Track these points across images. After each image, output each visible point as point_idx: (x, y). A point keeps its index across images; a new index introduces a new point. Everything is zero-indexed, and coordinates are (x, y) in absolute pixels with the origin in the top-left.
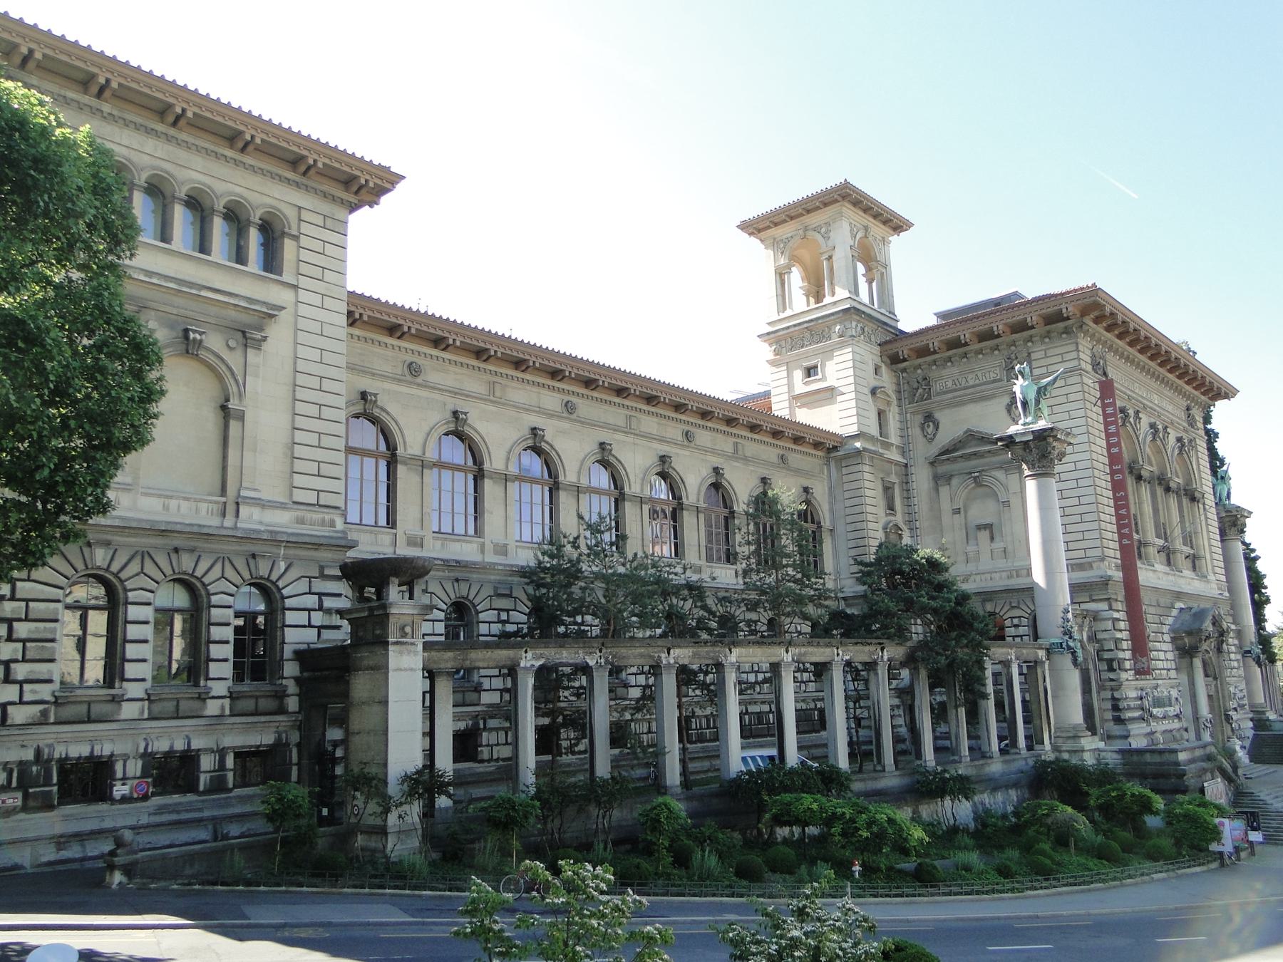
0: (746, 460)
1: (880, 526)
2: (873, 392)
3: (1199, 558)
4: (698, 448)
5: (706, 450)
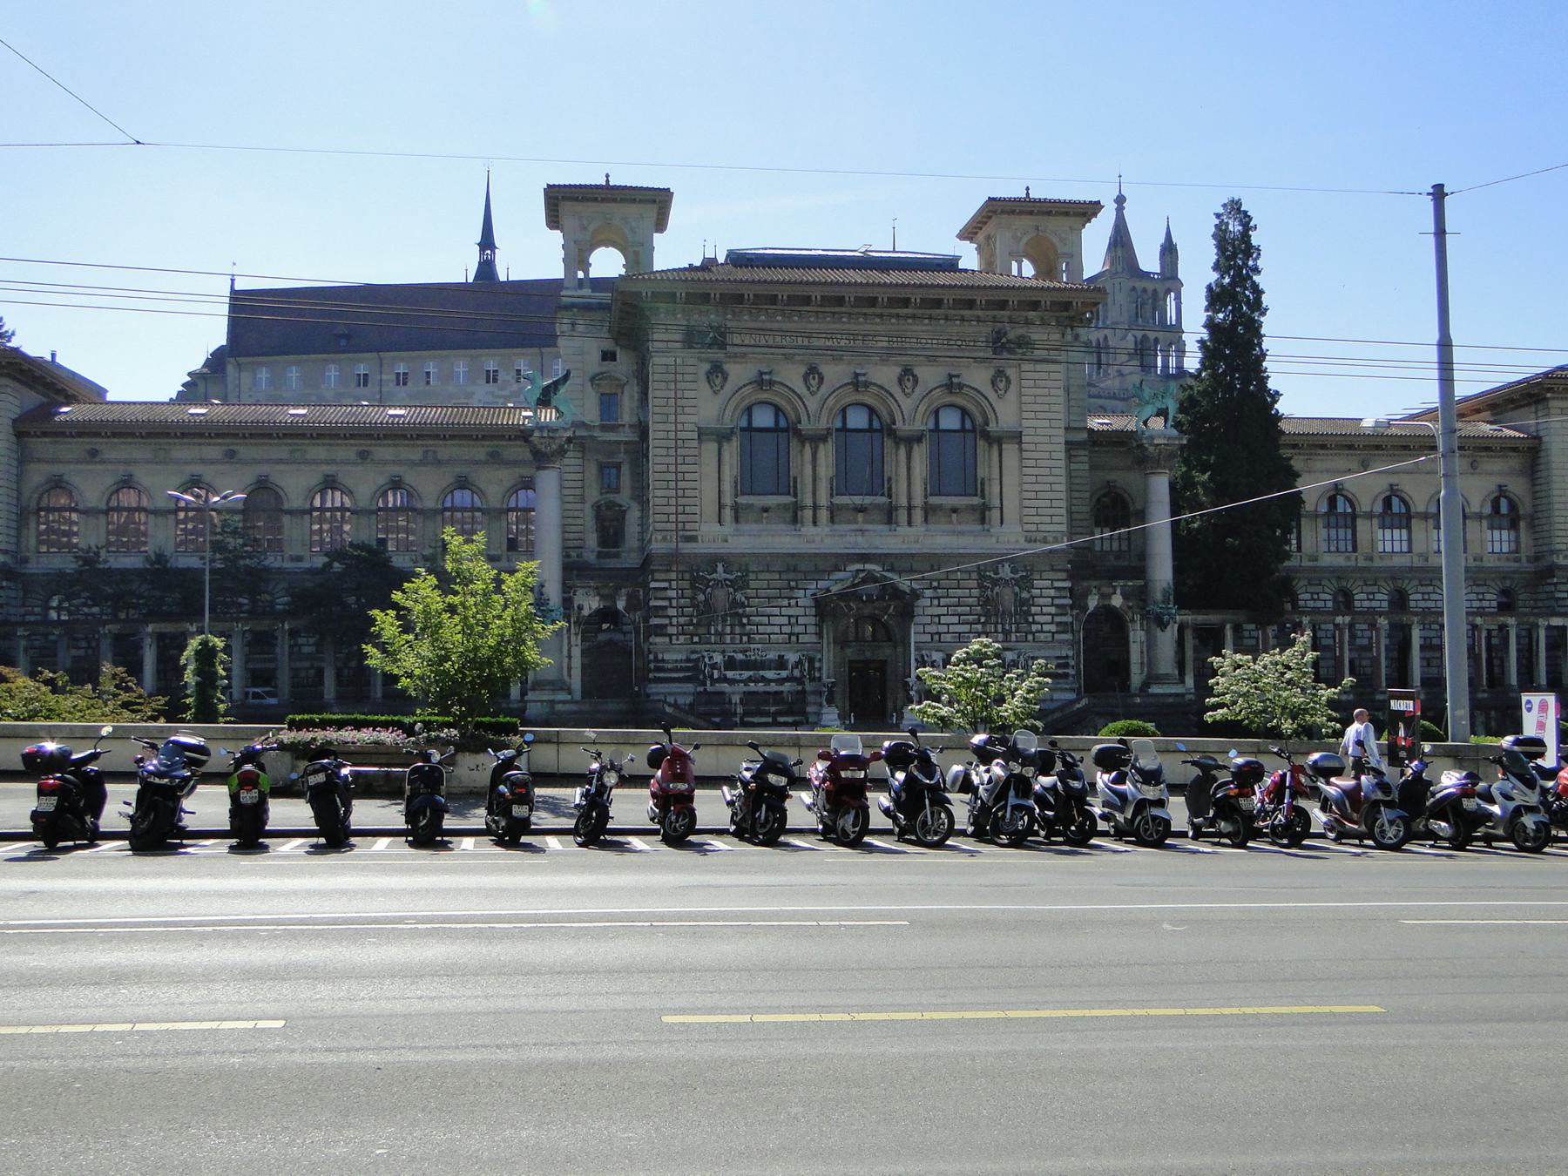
0: (438, 463)
1: (588, 508)
2: (592, 380)
3: (990, 509)
4: (374, 462)
5: (385, 462)
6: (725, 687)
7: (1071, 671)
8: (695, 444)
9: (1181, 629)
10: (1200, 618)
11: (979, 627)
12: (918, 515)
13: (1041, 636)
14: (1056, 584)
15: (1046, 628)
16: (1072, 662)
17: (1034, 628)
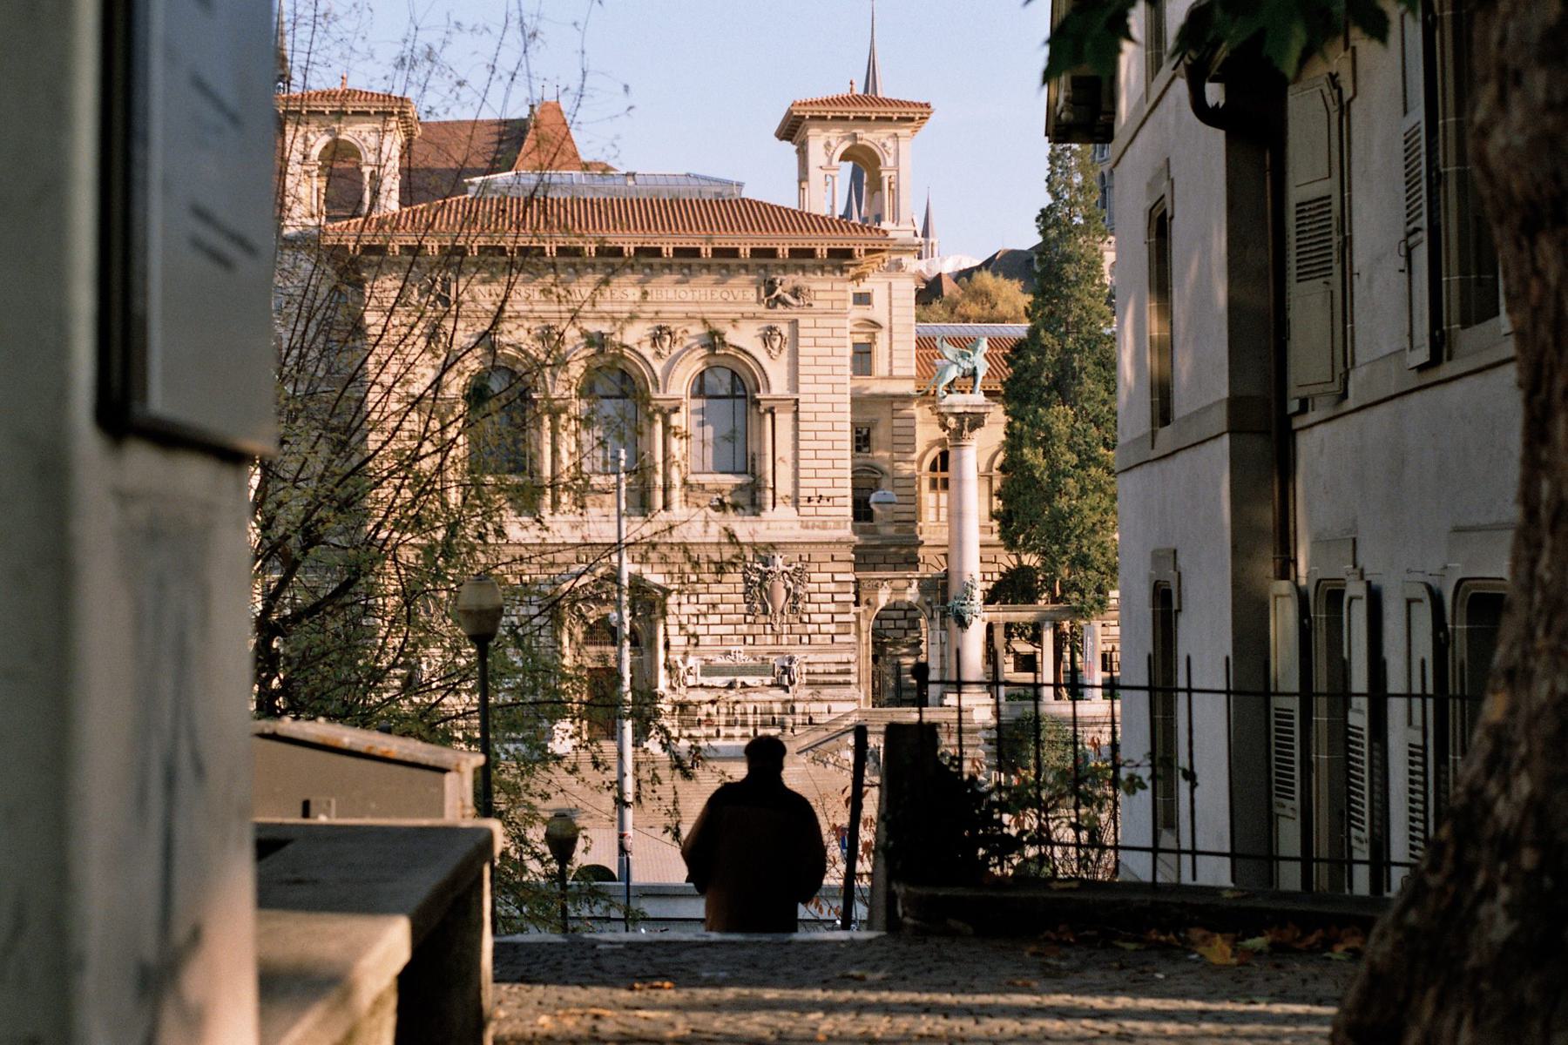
7: (853, 679)
9: (990, 628)
10: (1013, 617)
11: (744, 628)
12: (676, 495)
13: (818, 638)
14: (838, 577)
15: (824, 628)
16: (854, 668)
17: (810, 628)
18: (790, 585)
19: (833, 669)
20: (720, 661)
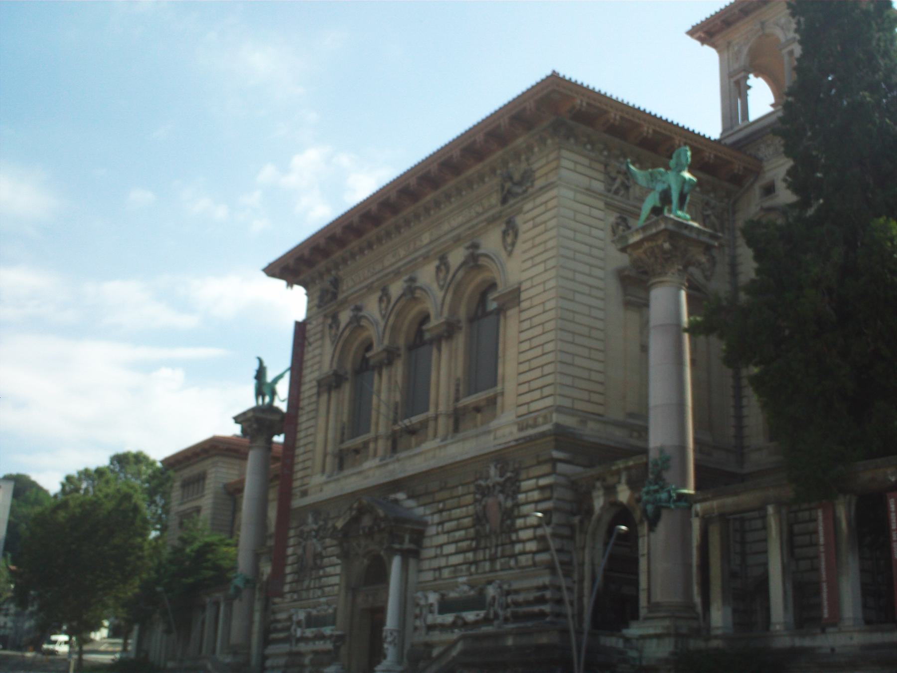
6: (302, 647)
8: (314, 399)
13: (523, 560)
16: (548, 594)
18: (501, 497)
19: (531, 596)
20: (453, 595)
